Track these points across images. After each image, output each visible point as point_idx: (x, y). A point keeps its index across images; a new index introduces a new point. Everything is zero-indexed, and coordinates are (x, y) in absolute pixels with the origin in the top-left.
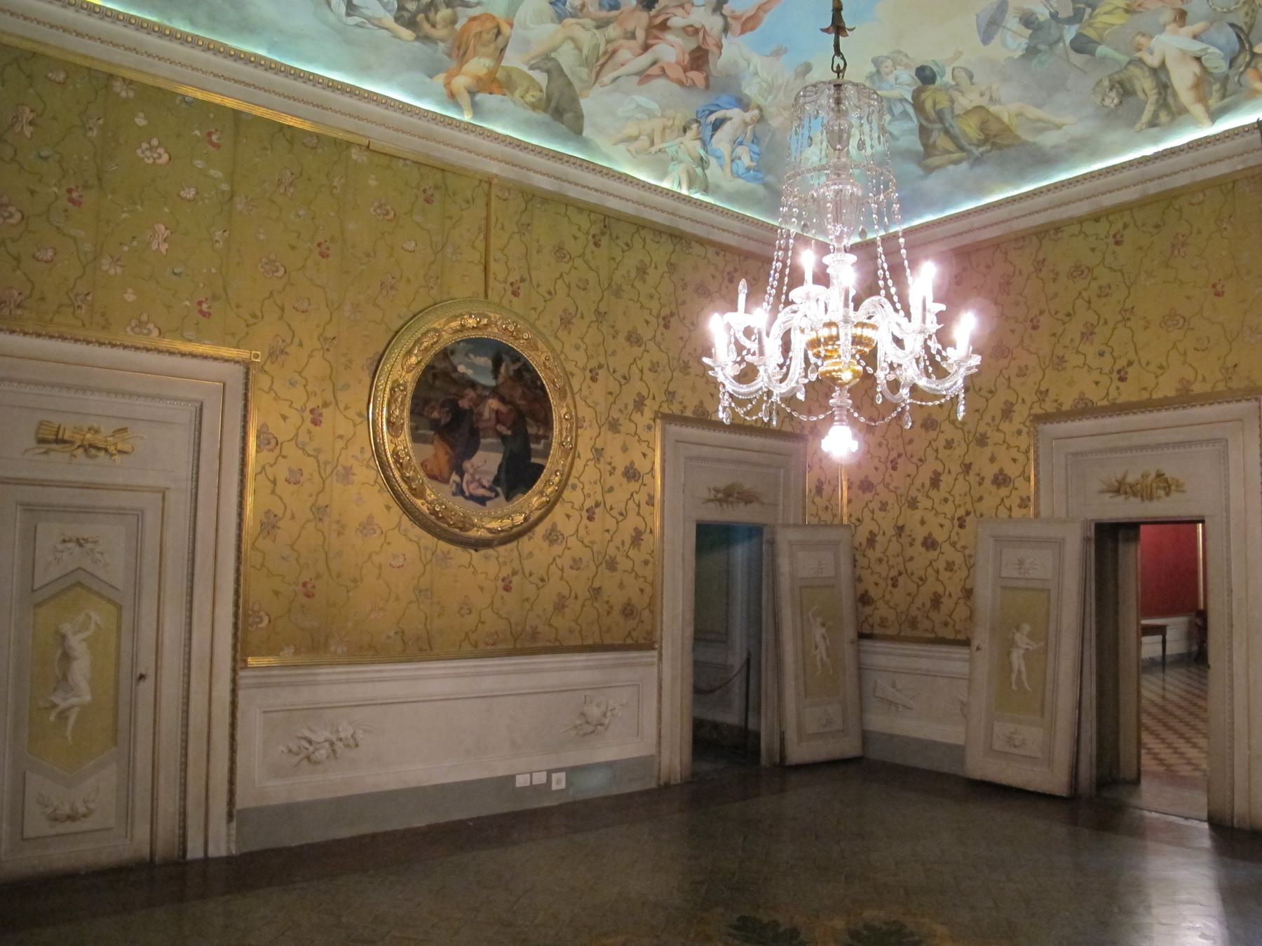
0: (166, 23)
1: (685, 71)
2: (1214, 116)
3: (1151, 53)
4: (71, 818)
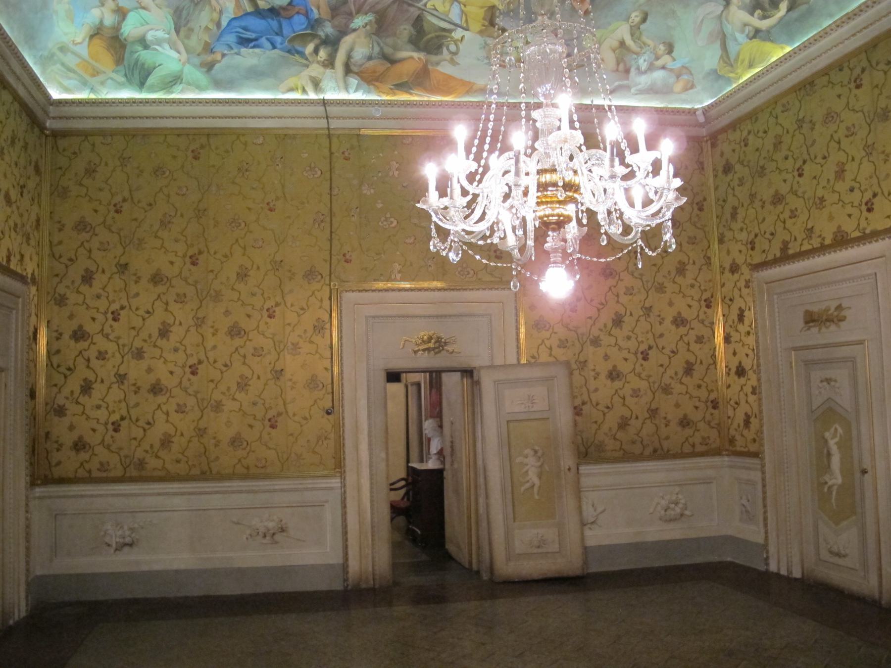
4: (838, 555)
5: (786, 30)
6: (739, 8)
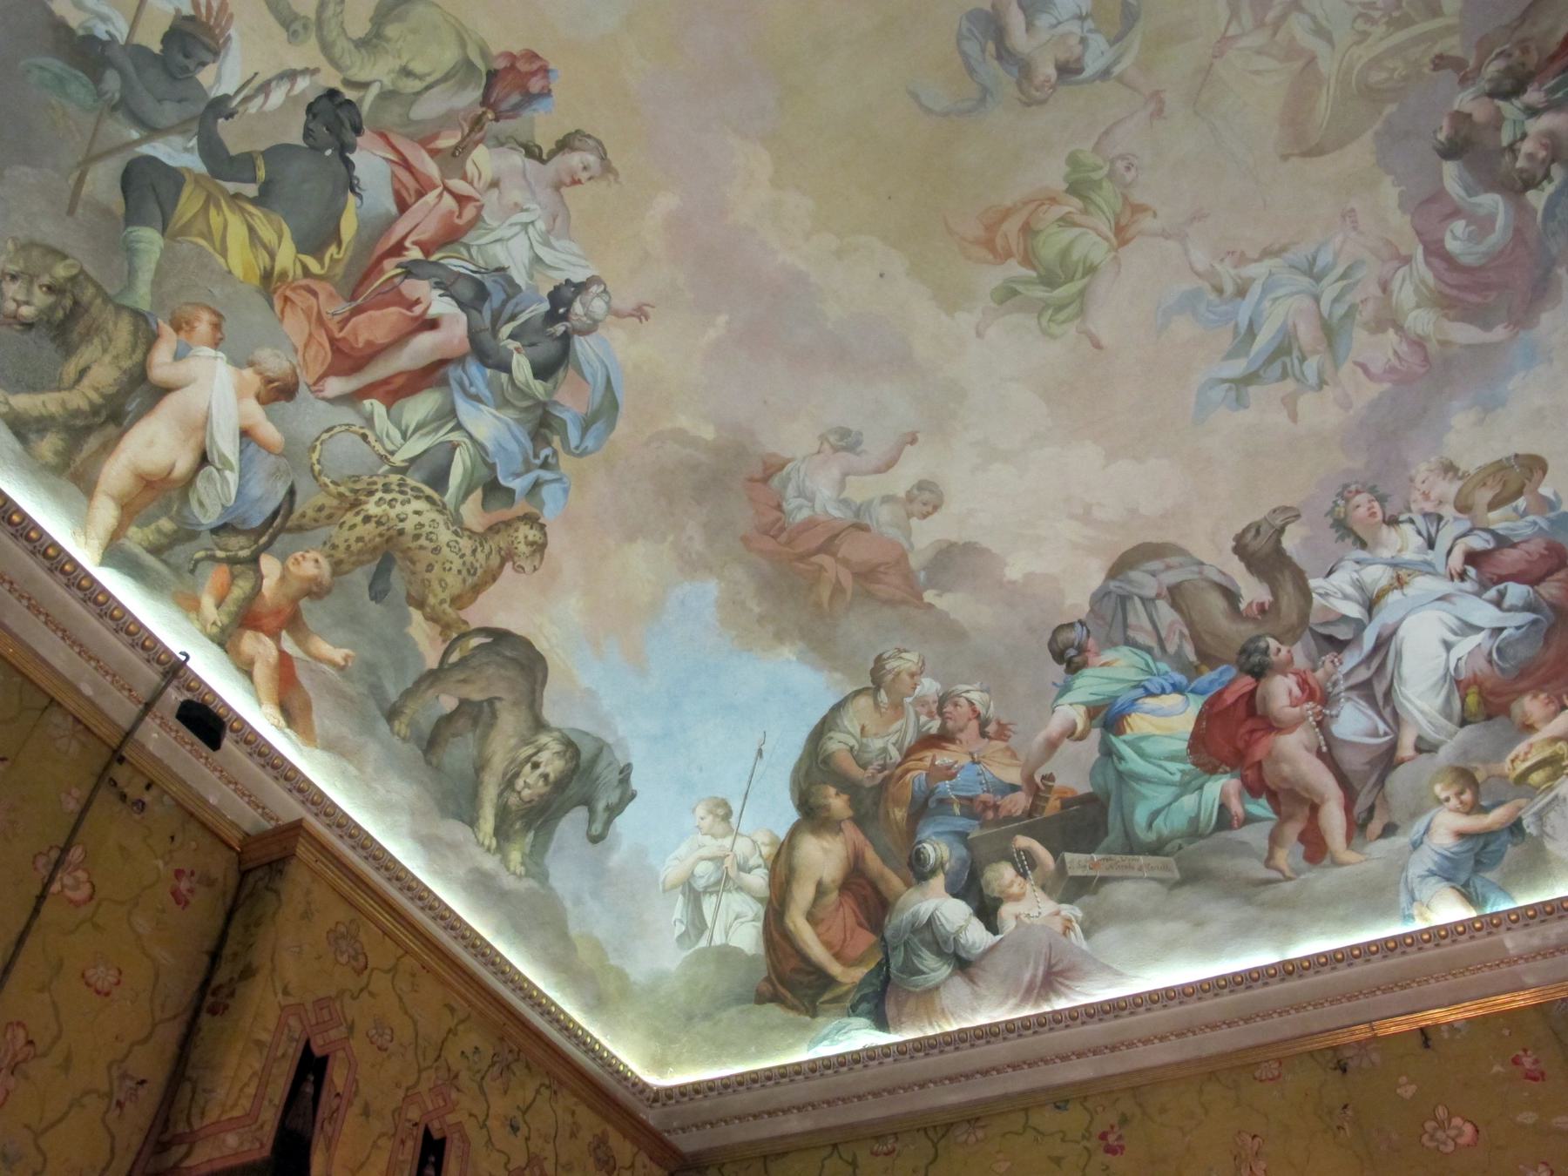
2: (114, 554)
3: (178, 356)
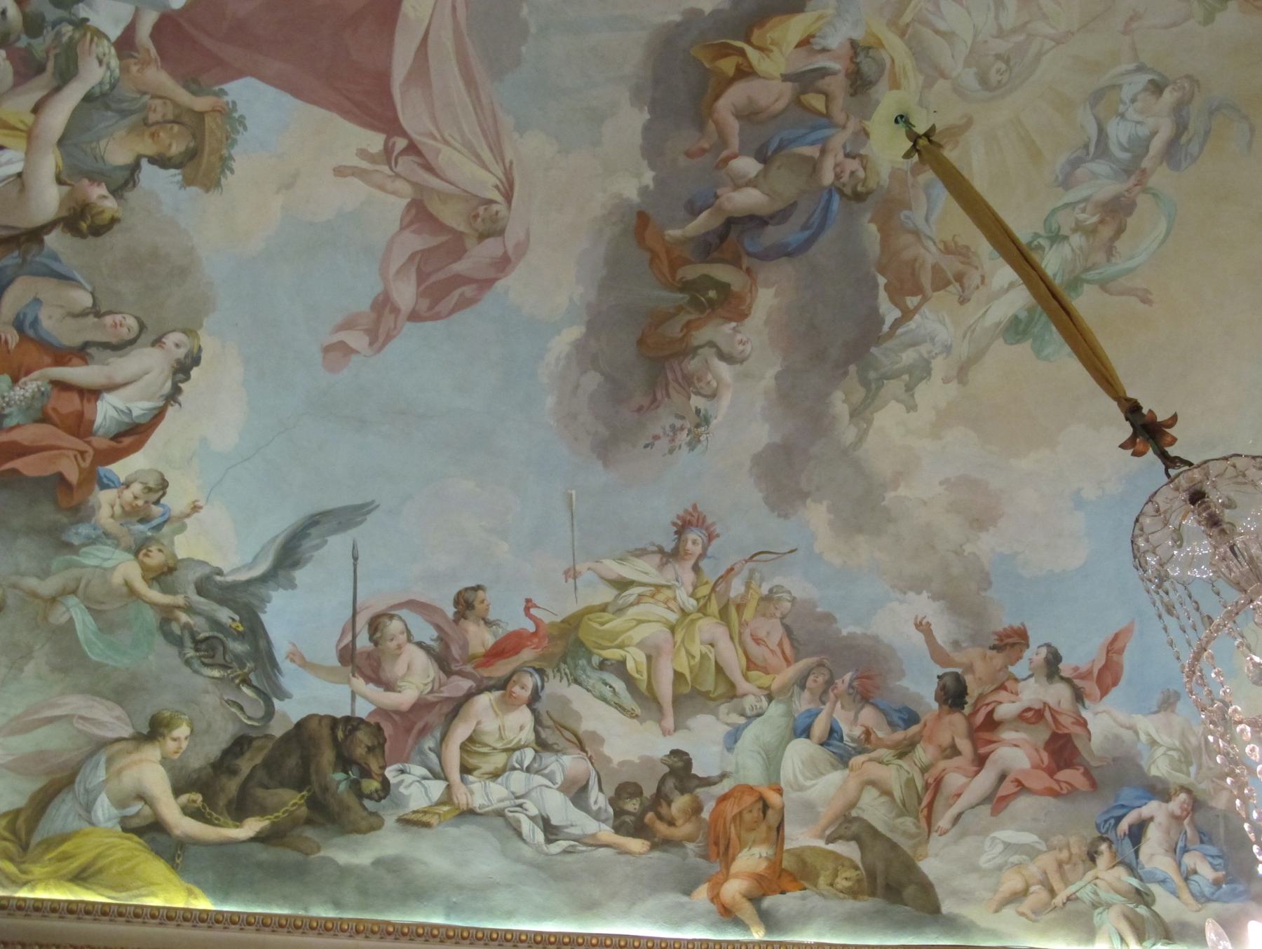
0: (301, 913)
1: (1051, 774)
5: (222, 867)
6: (165, 761)
